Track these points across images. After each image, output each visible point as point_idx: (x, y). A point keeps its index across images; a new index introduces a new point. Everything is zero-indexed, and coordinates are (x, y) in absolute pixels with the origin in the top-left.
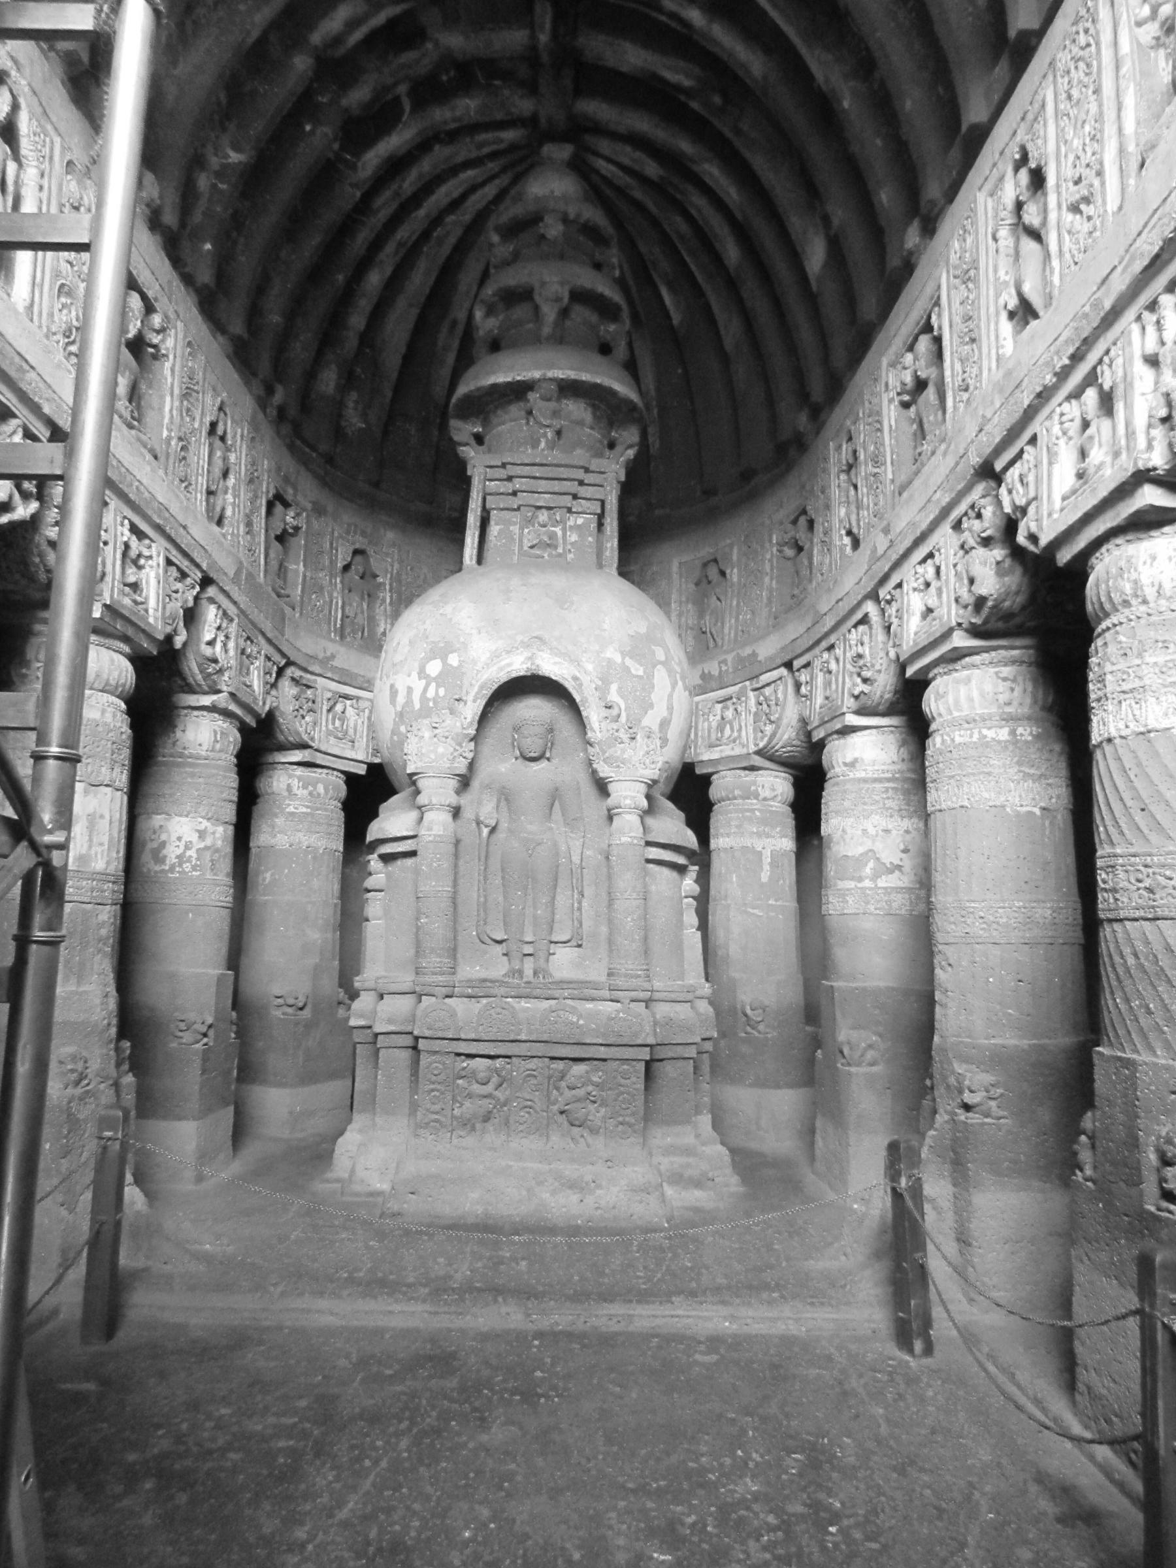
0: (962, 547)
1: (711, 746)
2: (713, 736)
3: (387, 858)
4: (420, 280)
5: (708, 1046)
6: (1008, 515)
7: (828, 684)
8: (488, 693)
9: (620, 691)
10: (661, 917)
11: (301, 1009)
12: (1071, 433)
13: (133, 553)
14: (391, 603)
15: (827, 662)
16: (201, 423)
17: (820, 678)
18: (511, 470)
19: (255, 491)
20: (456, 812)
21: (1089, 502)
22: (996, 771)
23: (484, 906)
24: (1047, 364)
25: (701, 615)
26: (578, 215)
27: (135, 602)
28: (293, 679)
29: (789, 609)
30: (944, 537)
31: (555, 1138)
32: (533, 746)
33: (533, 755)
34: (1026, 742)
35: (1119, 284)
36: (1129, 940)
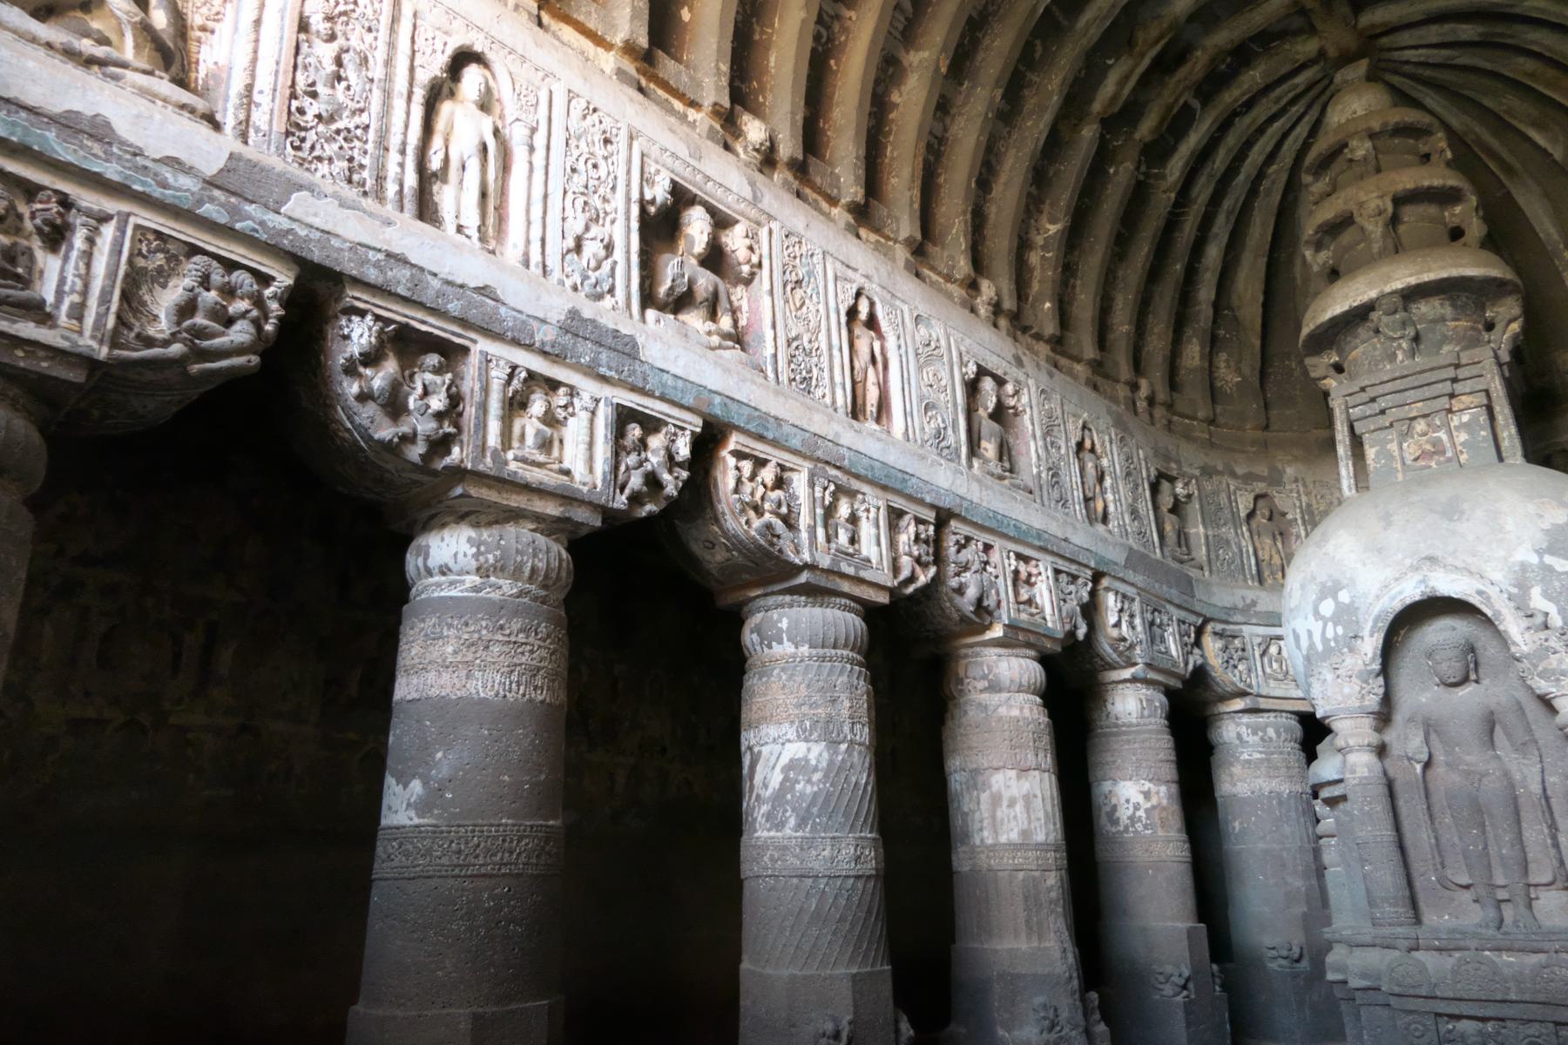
3: (1332, 802)
4: (1259, 231)
8: (1384, 625)
9: (1546, 595)
11: (1298, 961)
13: (1023, 575)
16: (1066, 447)
18: (1371, 393)
20: (1381, 751)
26: (1385, 124)
27: (1032, 615)
28: (1215, 634)
33: (1452, 680)
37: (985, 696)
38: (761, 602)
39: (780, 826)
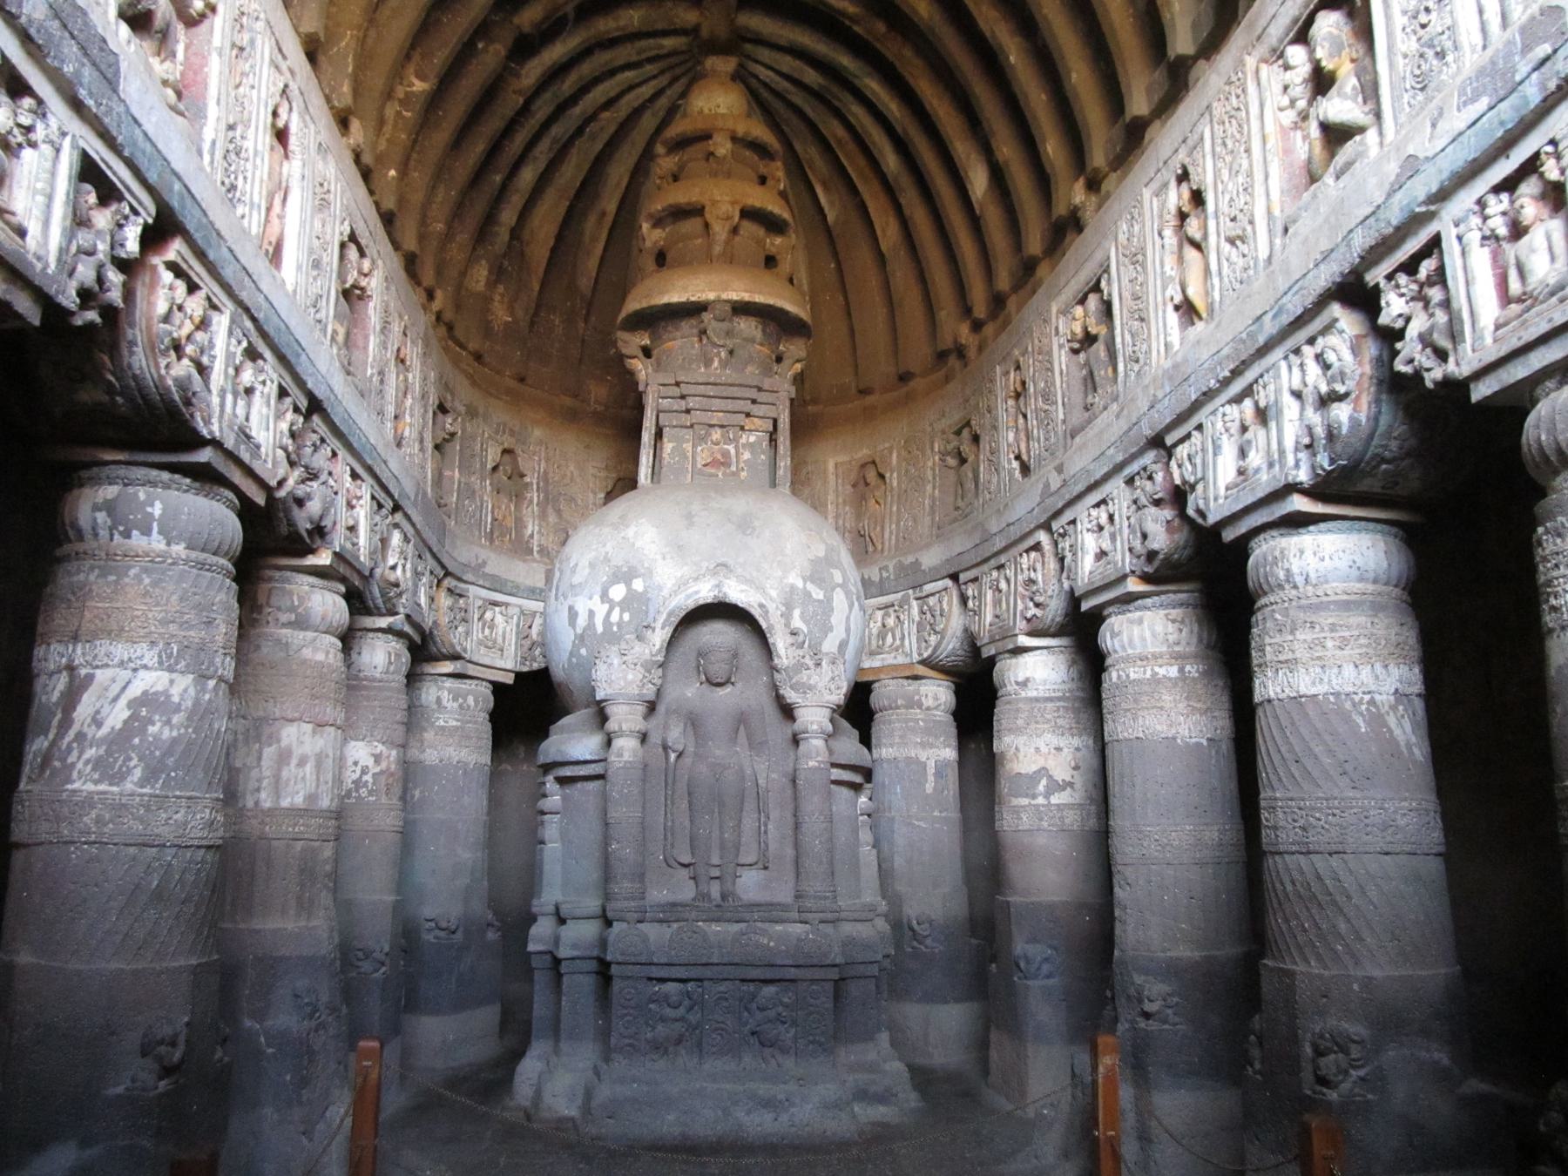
0: (1135, 502)
1: (872, 654)
2: (874, 643)
3: (562, 781)
4: (571, 173)
5: (887, 963)
6: (1177, 487)
7: (997, 603)
8: (675, 620)
9: (802, 616)
10: (842, 837)
12: (1232, 431)
15: (998, 581)
17: (989, 594)
18: (685, 389)
19: (425, 406)
20: (644, 738)
21: (1250, 500)
22: (1168, 705)
23: (669, 832)
24: (1212, 370)
25: (859, 517)
29: (955, 520)
30: (1116, 487)
31: (747, 1059)
32: (718, 670)
35: (1270, 327)
36: (1288, 869)
37: (284, 631)
38: (122, 471)
39: (118, 778)
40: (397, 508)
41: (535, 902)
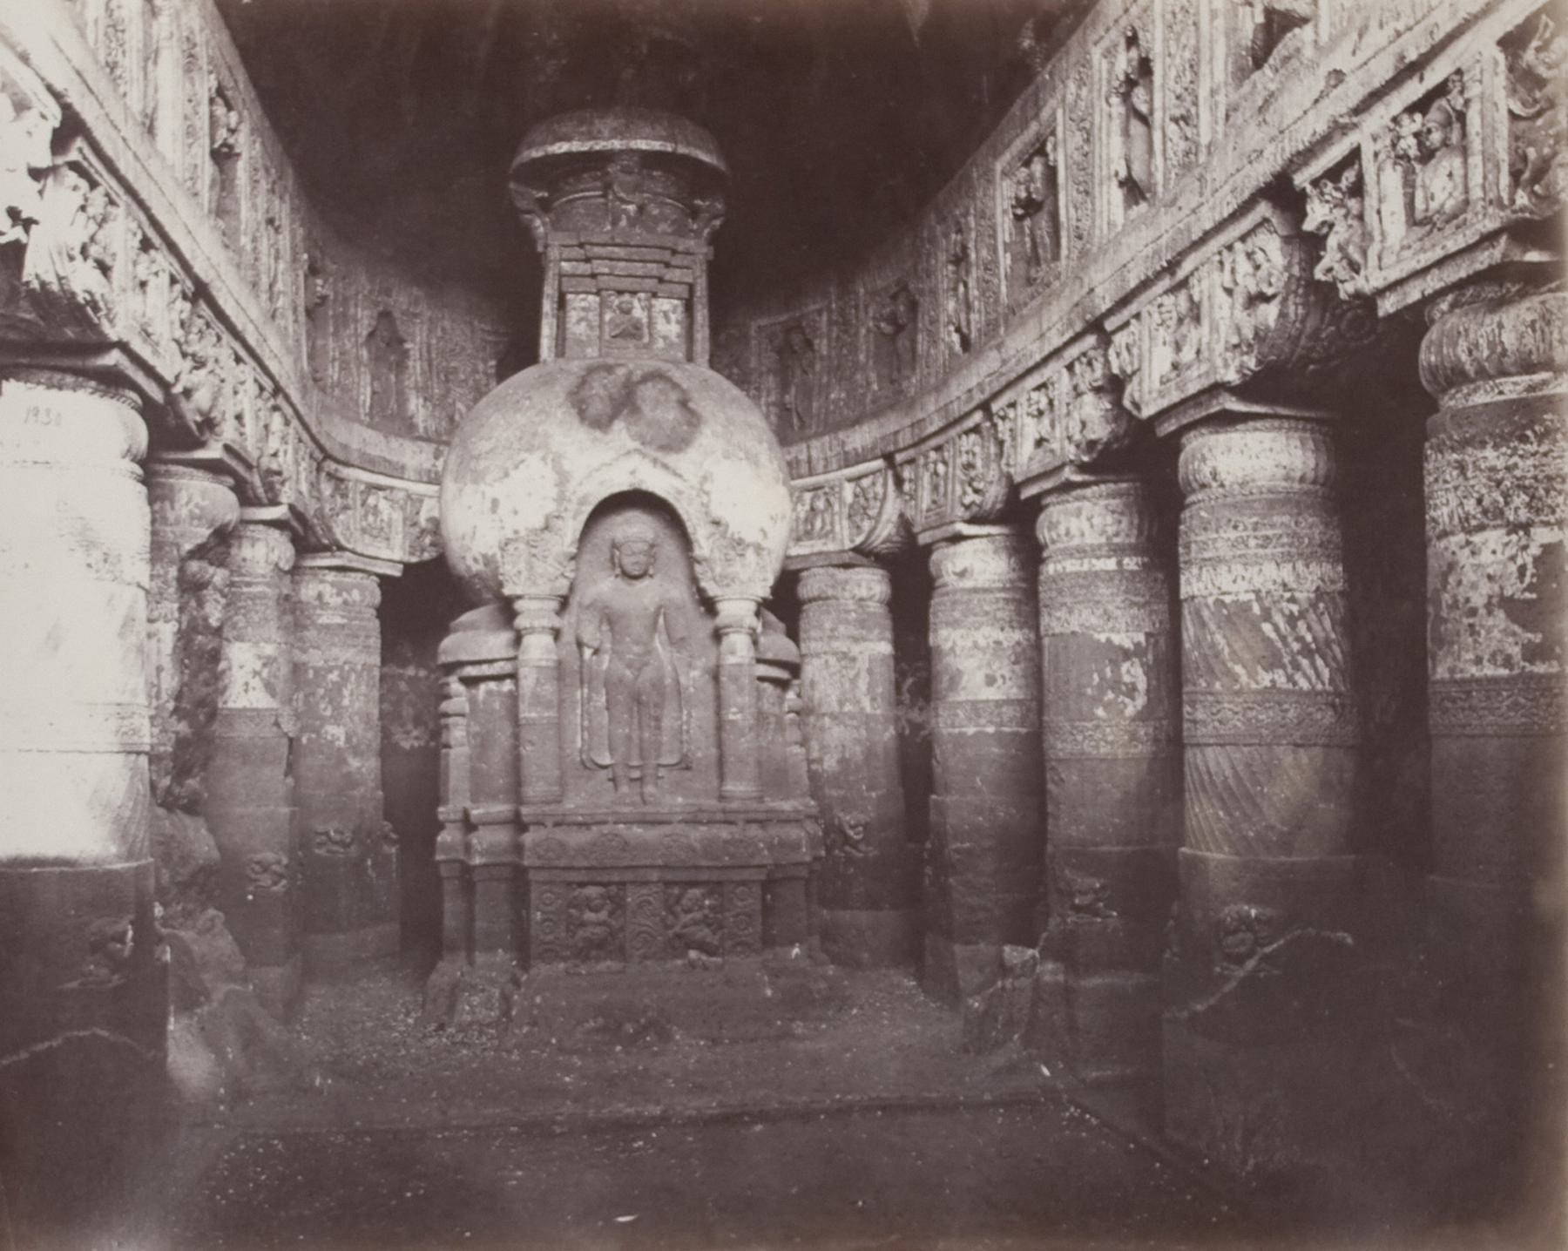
5: (817, 867)
6: (1116, 376)
7: (935, 488)
8: (588, 509)
14: (423, 372)
20: (557, 634)
28: (329, 474)
30: (1055, 370)
34: (1132, 572)
40: (278, 390)
41: (441, 809)
